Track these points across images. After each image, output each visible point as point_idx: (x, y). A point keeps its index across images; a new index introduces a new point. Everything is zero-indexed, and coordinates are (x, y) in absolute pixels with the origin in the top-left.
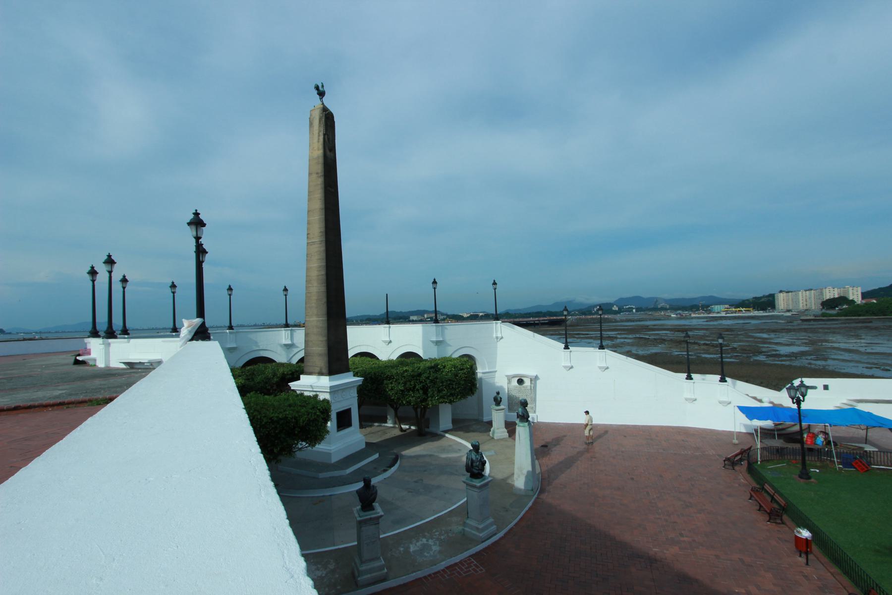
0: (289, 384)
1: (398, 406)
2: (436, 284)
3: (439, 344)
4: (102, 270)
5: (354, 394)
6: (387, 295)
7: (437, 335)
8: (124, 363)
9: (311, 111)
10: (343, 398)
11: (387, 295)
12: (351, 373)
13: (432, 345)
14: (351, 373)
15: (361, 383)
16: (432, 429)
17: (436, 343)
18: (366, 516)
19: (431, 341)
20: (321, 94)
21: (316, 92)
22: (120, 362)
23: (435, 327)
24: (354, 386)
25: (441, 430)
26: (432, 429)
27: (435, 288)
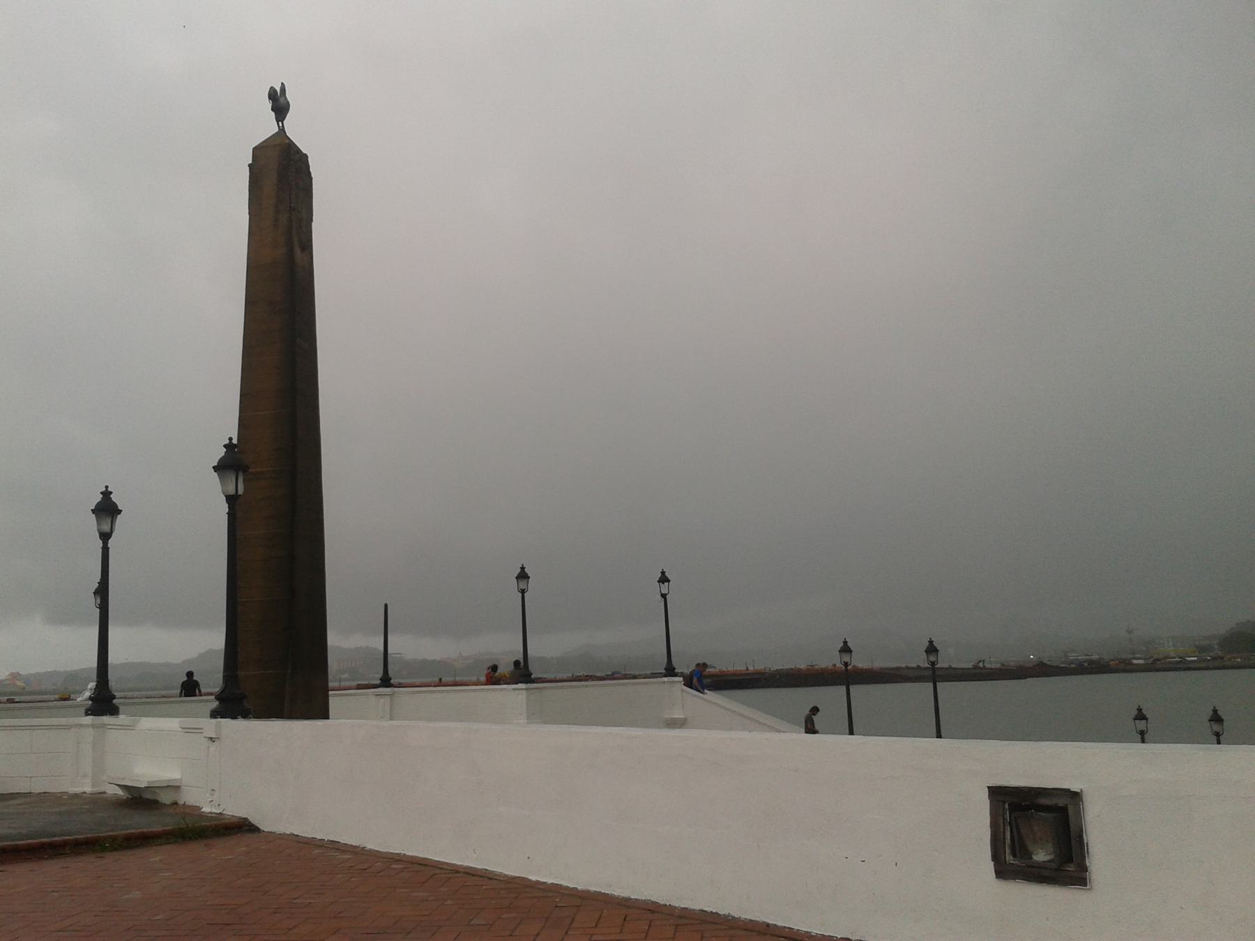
2: (525, 581)
6: (386, 606)
9: (253, 149)
11: (386, 606)
21: (269, 105)
23: (525, 691)
27: (523, 592)
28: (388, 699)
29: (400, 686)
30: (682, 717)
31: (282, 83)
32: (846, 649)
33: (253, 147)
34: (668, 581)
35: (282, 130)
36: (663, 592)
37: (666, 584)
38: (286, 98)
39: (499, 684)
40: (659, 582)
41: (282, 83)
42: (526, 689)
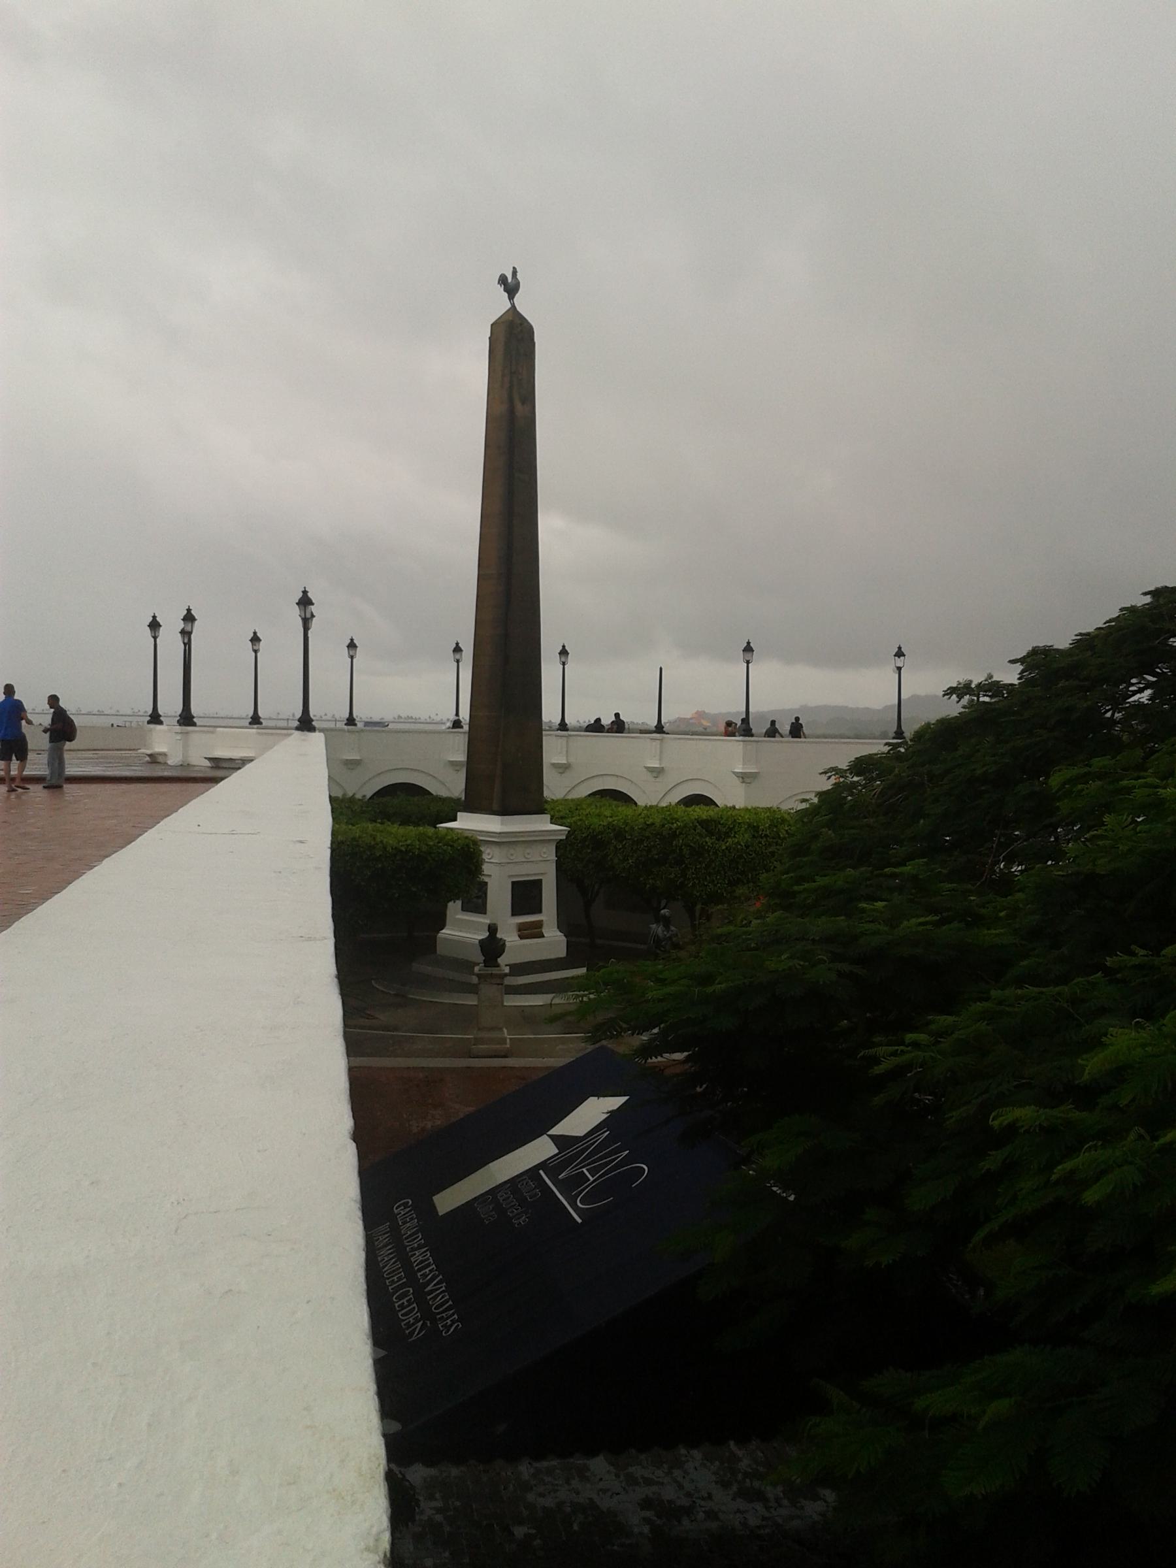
2: (750, 654)
3: (748, 780)
4: (172, 626)
6: (661, 669)
7: (745, 762)
8: (210, 759)
9: (492, 325)
10: (526, 858)
11: (661, 669)
12: (547, 817)
13: (737, 781)
14: (547, 817)
15: (564, 837)
17: (743, 778)
18: (487, 971)
19: (734, 773)
20: (511, 287)
22: (206, 758)
23: (742, 743)
24: (550, 841)
31: (514, 268)
33: (492, 322)
34: (904, 655)
35: (513, 306)
36: (898, 665)
37: (902, 658)
38: (517, 279)
39: (735, 736)
40: (895, 656)
41: (514, 268)
42: (742, 741)
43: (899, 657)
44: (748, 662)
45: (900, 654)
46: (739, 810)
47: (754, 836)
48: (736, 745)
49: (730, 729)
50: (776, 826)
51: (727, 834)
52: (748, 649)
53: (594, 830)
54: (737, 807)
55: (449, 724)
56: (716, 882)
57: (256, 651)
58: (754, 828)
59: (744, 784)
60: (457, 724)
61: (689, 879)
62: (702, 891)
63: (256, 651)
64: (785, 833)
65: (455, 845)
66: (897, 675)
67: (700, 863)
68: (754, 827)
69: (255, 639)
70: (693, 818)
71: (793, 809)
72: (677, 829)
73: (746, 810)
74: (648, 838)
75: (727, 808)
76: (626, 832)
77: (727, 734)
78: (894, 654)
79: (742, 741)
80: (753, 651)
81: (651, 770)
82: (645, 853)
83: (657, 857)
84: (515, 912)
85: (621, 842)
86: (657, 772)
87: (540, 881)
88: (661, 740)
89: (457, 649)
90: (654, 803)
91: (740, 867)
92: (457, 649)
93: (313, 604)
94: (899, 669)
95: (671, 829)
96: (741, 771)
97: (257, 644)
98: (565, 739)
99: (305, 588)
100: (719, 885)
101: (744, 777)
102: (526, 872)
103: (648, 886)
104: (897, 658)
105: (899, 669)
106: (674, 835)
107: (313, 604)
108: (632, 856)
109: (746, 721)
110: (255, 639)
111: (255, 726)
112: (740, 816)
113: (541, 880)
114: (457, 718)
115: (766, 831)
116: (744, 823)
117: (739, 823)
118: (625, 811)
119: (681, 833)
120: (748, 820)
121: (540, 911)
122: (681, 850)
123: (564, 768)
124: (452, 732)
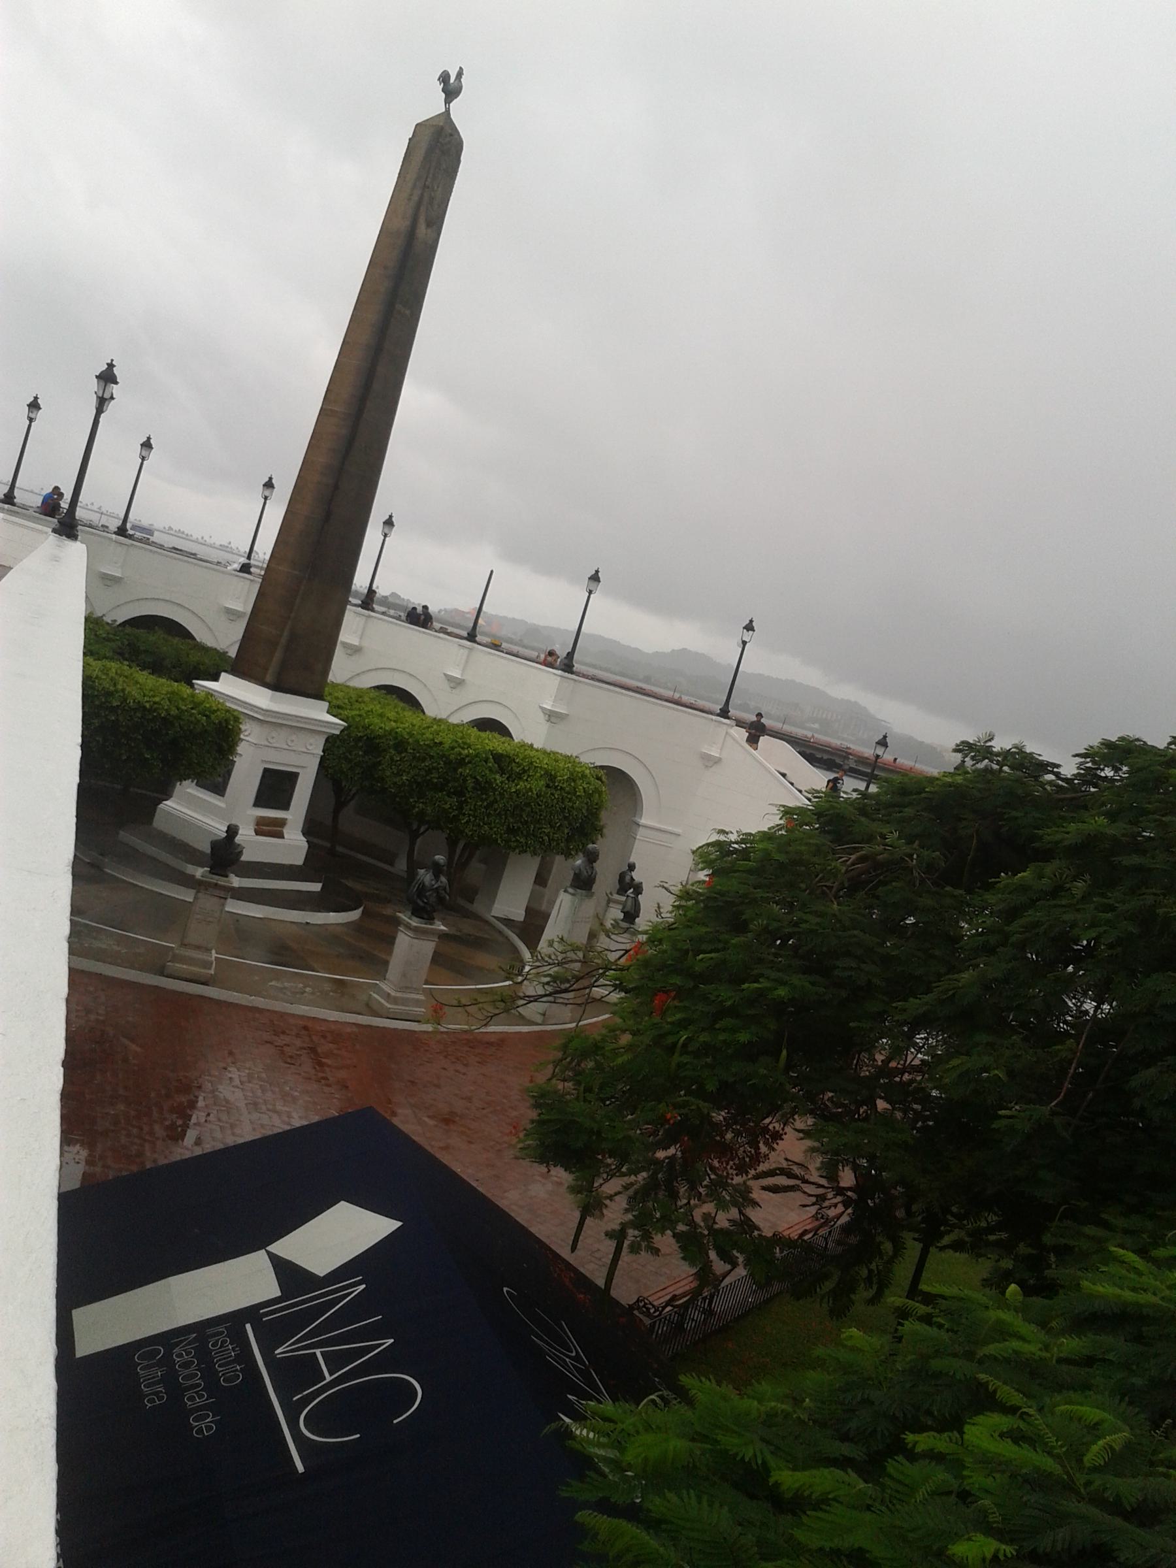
0: (194, 681)
1: (422, 829)
3: (553, 719)
5: (317, 747)
6: (492, 572)
11: (492, 572)
12: (325, 705)
13: (541, 718)
14: (325, 705)
15: (337, 732)
16: (478, 907)
17: (549, 716)
19: (542, 708)
23: (559, 678)
25: (493, 914)
26: (478, 907)
28: (466, 651)
29: (578, 674)
30: (718, 755)
32: (883, 743)
34: (754, 631)
37: (751, 632)
40: (744, 628)
42: (561, 676)
43: (748, 631)
44: (590, 592)
45: (749, 627)
46: (537, 750)
47: (548, 786)
48: (551, 678)
49: (550, 660)
50: (574, 781)
51: (519, 777)
52: (595, 578)
53: (372, 731)
54: (535, 746)
55: (237, 566)
56: (493, 825)
57: (31, 420)
58: (550, 777)
59: (549, 723)
60: (245, 568)
61: (464, 814)
62: (476, 831)
63: (31, 420)
64: (582, 791)
65: (213, 717)
66: (741, 649)
67: (482, 800)
68: (551, 775)
69: (34, 405)
70: (488, 748)
71: (594, 764)
72: (467, 756)
73: (545, 752)
74: (432, 757)
75: (523, 745)
76: (408, 743)
77: (546, 663)
78: (744, 625)
79: (561, 676)
80: (599, 581)
81: (449, 678)
82: (423, 773)
83: (436, 780)
84: (259, 802)
85: (400, 753)
86: (456, 683)
87: (298, 773)
88: (471, 649)
89: (269, 485)
90: (443, 715)
91: (524, 816)
92: (269, 485)
93: (116, 383)
94: (744, 643)
95: (460, 754)
96: (549, 708)
97: (35, 412)
98: (364, 618)
99: (112, 360)
100: (495, 829)
101: (552, 717)
102: (283, 761)
103: (417, 809)
104: (745, 630)
105: (744, 643)
106: (462, 762)
107: (116, 383)
108: (409, 773)
109: (570, 655)
110: (34, 405)
111: (6, 506)
112: (538, 758)
113: (298, 773)
114: (247, 561)
115: (563, 783)
116: (541, 767)
117: (535, 767)
118: (409, 716)
119: (470, 762)
120: (546, 766)
121: (285, 806)
122: (465, 781)
123: (355, 650)
124: (237, 576)
